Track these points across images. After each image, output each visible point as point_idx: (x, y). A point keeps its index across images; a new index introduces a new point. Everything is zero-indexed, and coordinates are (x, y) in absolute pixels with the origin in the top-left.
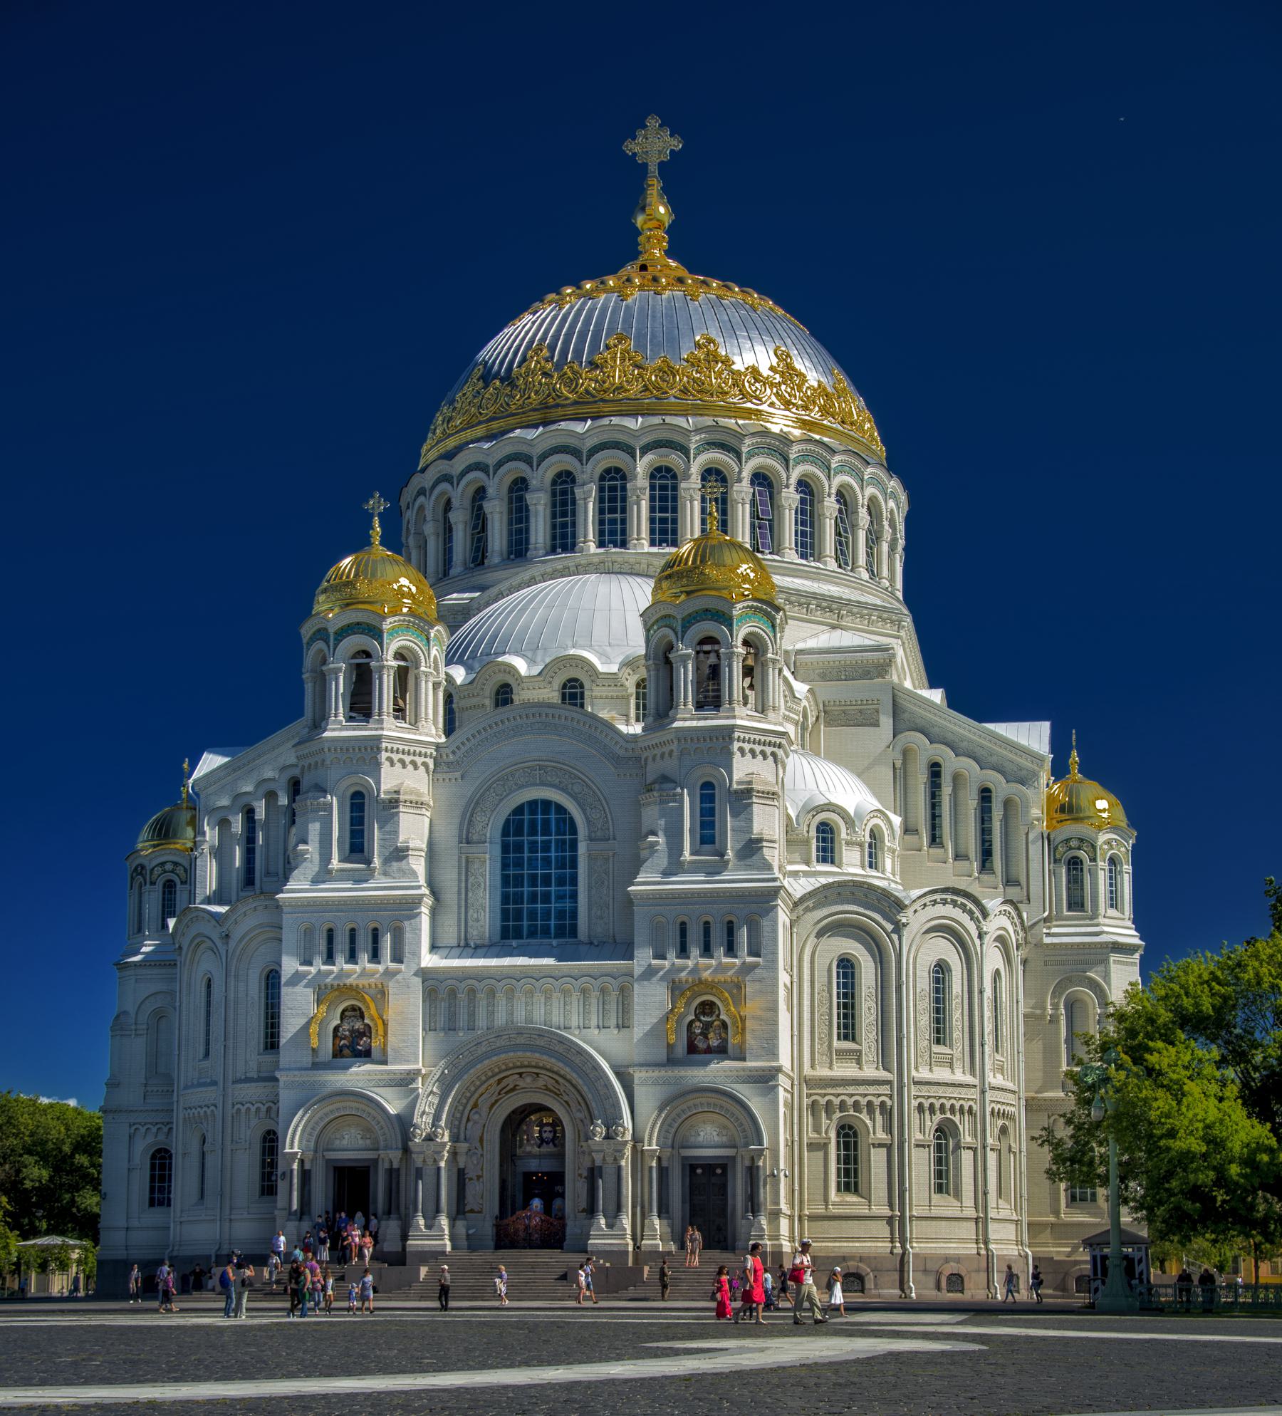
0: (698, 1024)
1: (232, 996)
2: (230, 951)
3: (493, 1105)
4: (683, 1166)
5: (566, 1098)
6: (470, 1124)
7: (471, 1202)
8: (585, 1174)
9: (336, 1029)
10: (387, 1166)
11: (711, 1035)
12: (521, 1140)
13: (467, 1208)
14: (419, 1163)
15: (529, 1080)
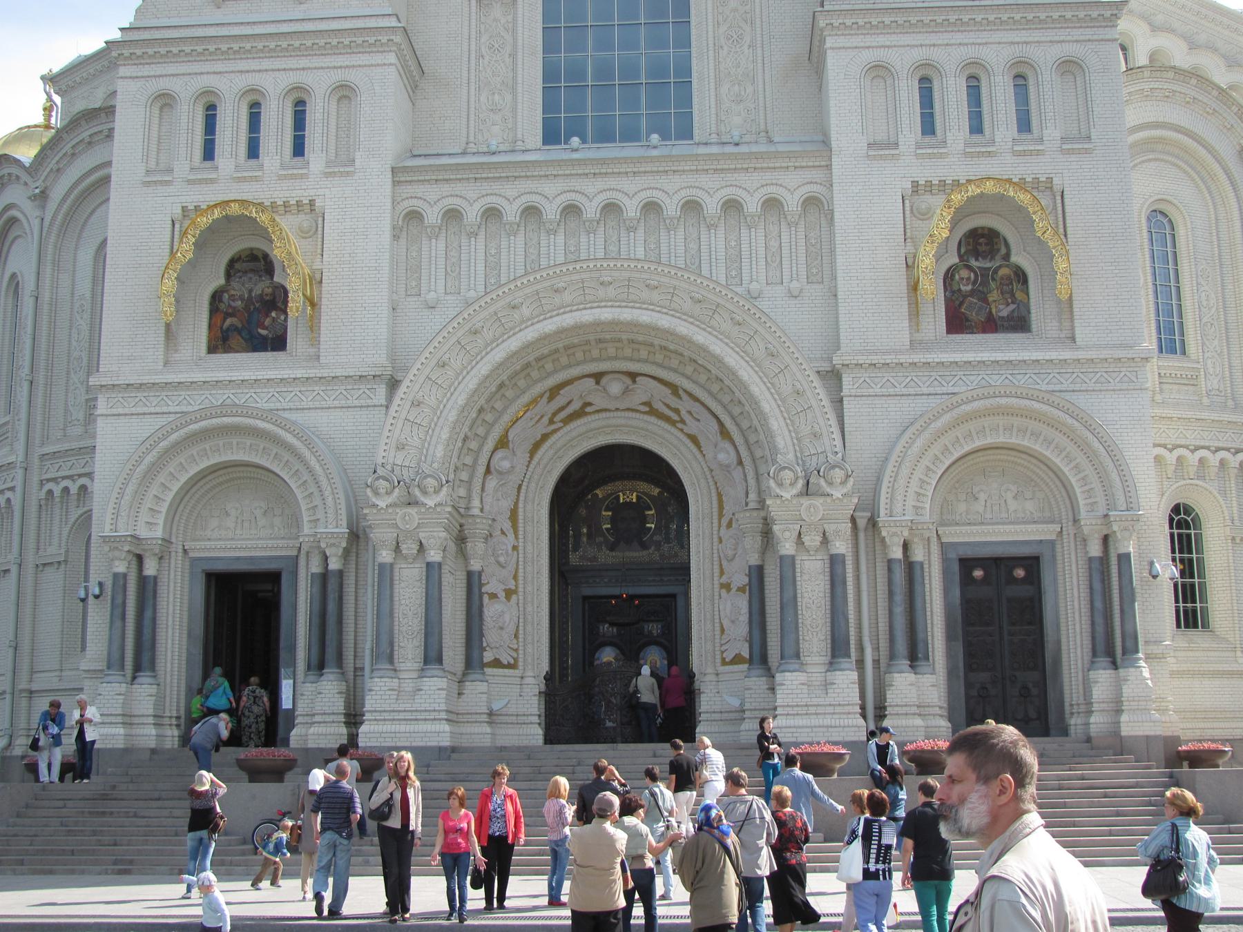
0: (964, 273)
1: (46, 296)
2: (46, 223)
3: (536, 446)
4: (945, 560)
5: (692, 427)
6: (492, 483)
7: (496, 641)
8: (741, 579)
9: (216, 297)
10: (316, 568)
11: (994, 296)
12: (577, 536)
13: (488, 656)
14: (386, 556)
15: (615, 387)
